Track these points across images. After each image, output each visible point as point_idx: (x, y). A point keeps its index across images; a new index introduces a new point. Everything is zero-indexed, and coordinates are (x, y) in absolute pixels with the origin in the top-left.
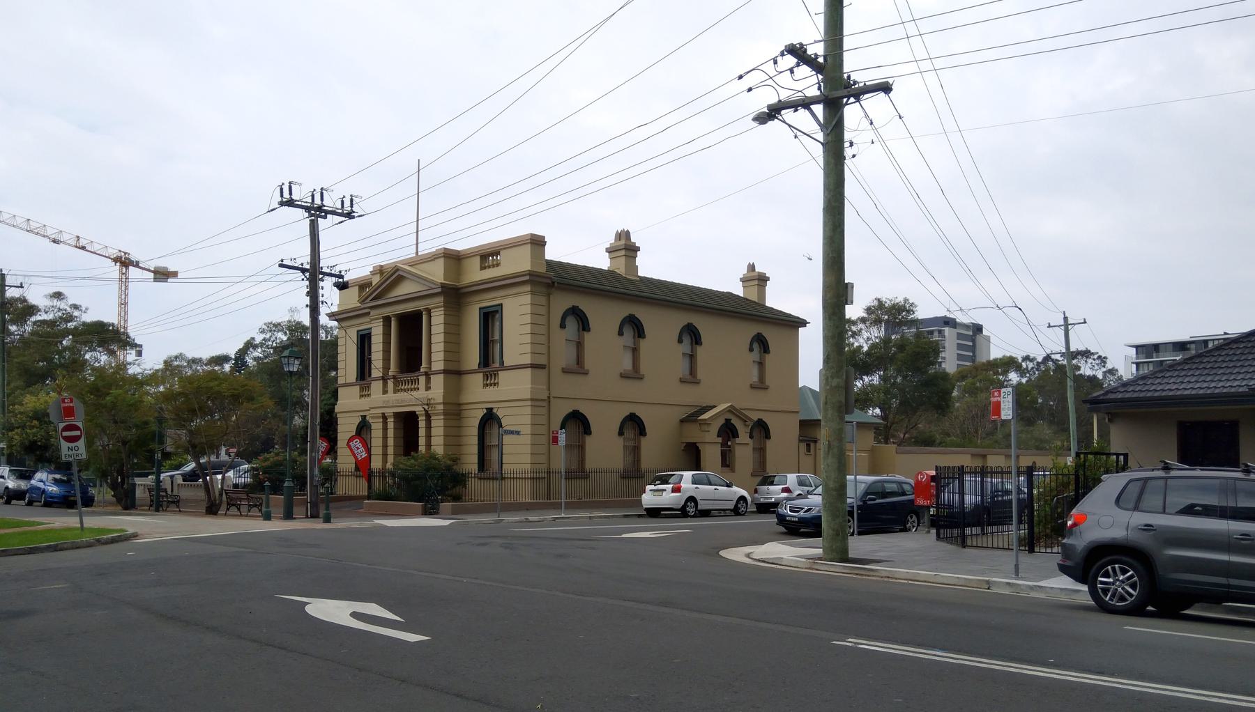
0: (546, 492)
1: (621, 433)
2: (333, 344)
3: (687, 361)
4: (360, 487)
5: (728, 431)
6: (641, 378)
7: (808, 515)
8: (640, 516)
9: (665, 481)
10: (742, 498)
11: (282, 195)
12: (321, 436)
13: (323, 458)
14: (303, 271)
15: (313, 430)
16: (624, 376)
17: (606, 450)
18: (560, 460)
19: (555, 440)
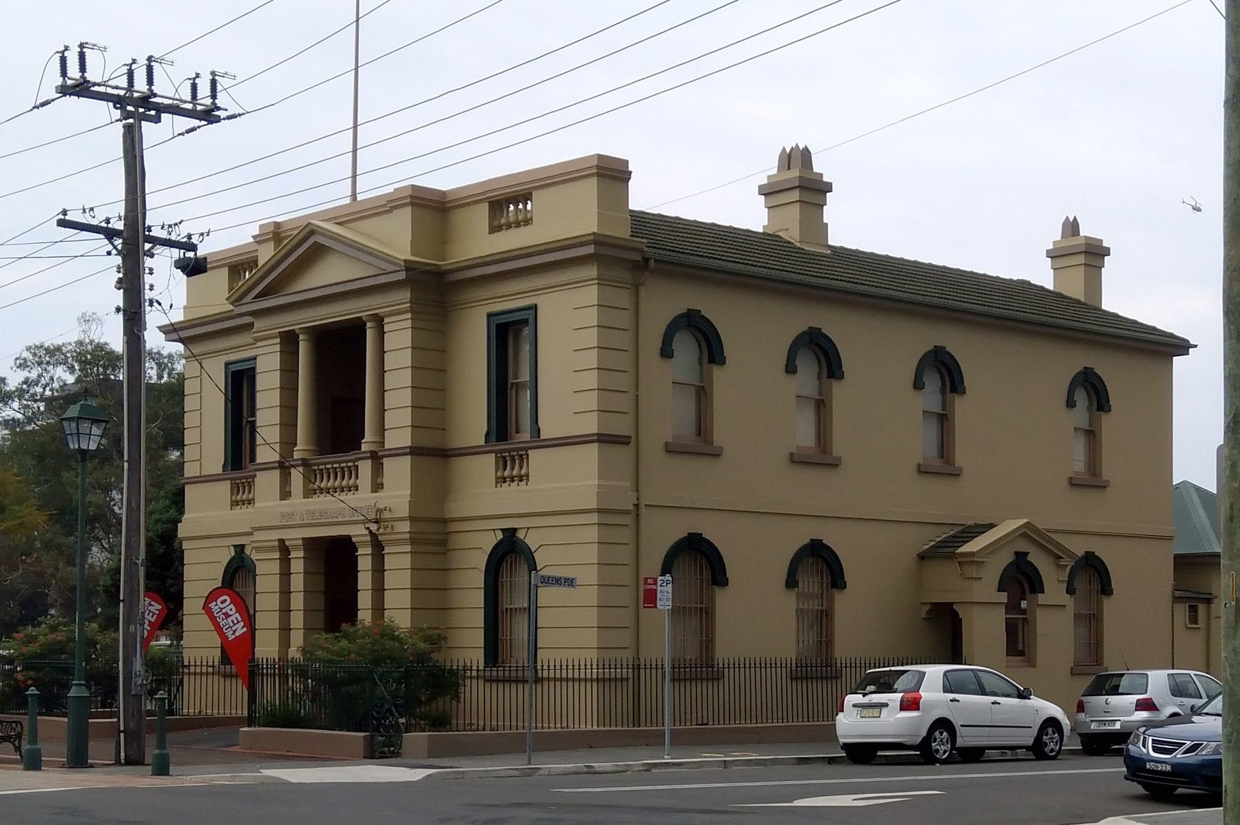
0: (631, 710)
1: (791, 583)
2: (174, 392)
3: (933, 427)
4: (230, 698)
5: (1021, 579)
6: (835, 465)
7: (1191, 758)
8: (832, 761)
9: (885, 685)
10: (1052, 722)
11: (64, 73)
12: (147, 589)
13: (152, 636)
14: (110, 234)
15: (132, 578)
16: (798, 460)
17: (758, 619)
18: (661, 639)
19: (651, 598)
